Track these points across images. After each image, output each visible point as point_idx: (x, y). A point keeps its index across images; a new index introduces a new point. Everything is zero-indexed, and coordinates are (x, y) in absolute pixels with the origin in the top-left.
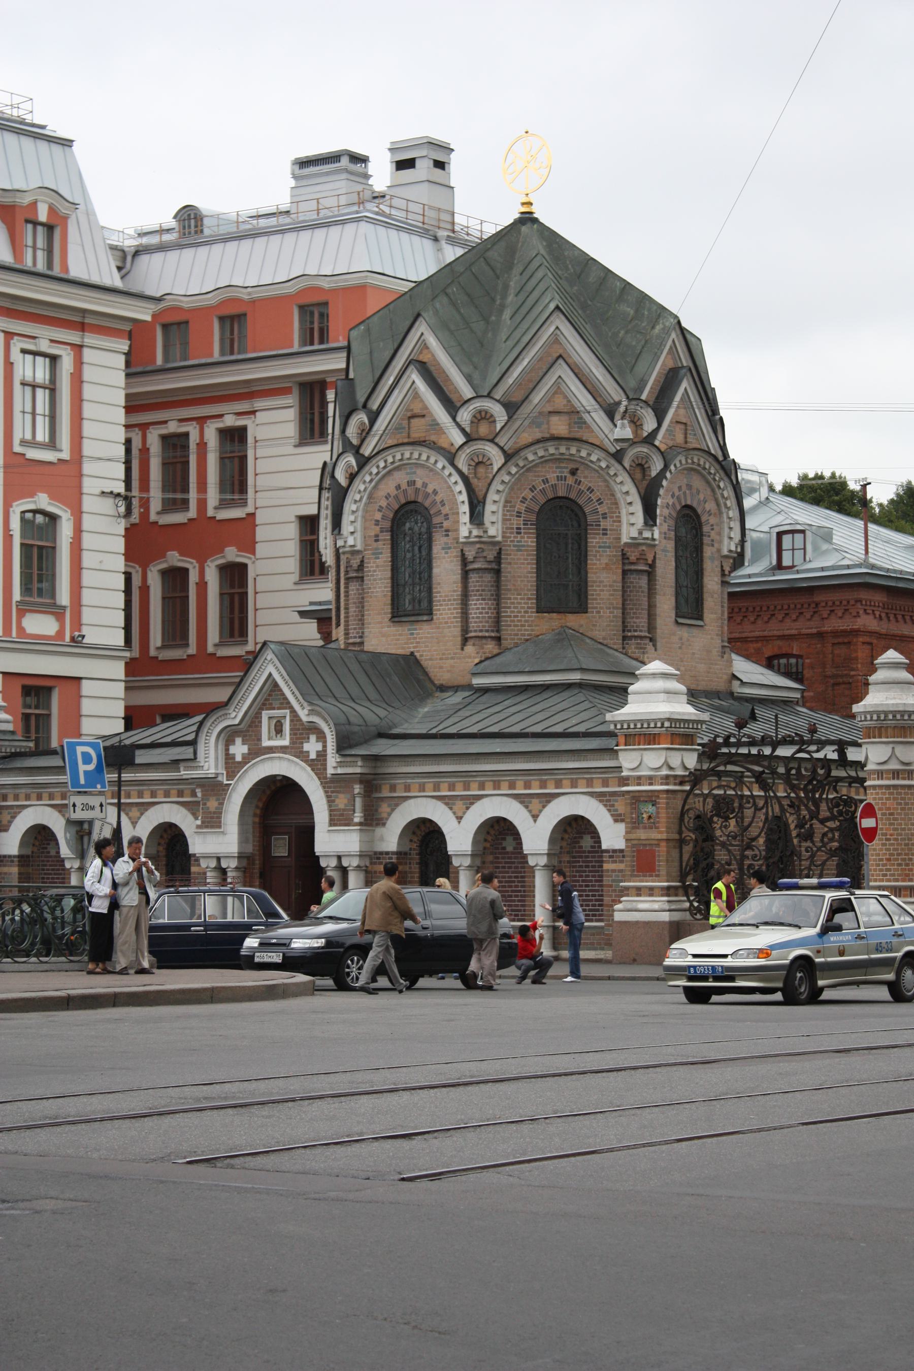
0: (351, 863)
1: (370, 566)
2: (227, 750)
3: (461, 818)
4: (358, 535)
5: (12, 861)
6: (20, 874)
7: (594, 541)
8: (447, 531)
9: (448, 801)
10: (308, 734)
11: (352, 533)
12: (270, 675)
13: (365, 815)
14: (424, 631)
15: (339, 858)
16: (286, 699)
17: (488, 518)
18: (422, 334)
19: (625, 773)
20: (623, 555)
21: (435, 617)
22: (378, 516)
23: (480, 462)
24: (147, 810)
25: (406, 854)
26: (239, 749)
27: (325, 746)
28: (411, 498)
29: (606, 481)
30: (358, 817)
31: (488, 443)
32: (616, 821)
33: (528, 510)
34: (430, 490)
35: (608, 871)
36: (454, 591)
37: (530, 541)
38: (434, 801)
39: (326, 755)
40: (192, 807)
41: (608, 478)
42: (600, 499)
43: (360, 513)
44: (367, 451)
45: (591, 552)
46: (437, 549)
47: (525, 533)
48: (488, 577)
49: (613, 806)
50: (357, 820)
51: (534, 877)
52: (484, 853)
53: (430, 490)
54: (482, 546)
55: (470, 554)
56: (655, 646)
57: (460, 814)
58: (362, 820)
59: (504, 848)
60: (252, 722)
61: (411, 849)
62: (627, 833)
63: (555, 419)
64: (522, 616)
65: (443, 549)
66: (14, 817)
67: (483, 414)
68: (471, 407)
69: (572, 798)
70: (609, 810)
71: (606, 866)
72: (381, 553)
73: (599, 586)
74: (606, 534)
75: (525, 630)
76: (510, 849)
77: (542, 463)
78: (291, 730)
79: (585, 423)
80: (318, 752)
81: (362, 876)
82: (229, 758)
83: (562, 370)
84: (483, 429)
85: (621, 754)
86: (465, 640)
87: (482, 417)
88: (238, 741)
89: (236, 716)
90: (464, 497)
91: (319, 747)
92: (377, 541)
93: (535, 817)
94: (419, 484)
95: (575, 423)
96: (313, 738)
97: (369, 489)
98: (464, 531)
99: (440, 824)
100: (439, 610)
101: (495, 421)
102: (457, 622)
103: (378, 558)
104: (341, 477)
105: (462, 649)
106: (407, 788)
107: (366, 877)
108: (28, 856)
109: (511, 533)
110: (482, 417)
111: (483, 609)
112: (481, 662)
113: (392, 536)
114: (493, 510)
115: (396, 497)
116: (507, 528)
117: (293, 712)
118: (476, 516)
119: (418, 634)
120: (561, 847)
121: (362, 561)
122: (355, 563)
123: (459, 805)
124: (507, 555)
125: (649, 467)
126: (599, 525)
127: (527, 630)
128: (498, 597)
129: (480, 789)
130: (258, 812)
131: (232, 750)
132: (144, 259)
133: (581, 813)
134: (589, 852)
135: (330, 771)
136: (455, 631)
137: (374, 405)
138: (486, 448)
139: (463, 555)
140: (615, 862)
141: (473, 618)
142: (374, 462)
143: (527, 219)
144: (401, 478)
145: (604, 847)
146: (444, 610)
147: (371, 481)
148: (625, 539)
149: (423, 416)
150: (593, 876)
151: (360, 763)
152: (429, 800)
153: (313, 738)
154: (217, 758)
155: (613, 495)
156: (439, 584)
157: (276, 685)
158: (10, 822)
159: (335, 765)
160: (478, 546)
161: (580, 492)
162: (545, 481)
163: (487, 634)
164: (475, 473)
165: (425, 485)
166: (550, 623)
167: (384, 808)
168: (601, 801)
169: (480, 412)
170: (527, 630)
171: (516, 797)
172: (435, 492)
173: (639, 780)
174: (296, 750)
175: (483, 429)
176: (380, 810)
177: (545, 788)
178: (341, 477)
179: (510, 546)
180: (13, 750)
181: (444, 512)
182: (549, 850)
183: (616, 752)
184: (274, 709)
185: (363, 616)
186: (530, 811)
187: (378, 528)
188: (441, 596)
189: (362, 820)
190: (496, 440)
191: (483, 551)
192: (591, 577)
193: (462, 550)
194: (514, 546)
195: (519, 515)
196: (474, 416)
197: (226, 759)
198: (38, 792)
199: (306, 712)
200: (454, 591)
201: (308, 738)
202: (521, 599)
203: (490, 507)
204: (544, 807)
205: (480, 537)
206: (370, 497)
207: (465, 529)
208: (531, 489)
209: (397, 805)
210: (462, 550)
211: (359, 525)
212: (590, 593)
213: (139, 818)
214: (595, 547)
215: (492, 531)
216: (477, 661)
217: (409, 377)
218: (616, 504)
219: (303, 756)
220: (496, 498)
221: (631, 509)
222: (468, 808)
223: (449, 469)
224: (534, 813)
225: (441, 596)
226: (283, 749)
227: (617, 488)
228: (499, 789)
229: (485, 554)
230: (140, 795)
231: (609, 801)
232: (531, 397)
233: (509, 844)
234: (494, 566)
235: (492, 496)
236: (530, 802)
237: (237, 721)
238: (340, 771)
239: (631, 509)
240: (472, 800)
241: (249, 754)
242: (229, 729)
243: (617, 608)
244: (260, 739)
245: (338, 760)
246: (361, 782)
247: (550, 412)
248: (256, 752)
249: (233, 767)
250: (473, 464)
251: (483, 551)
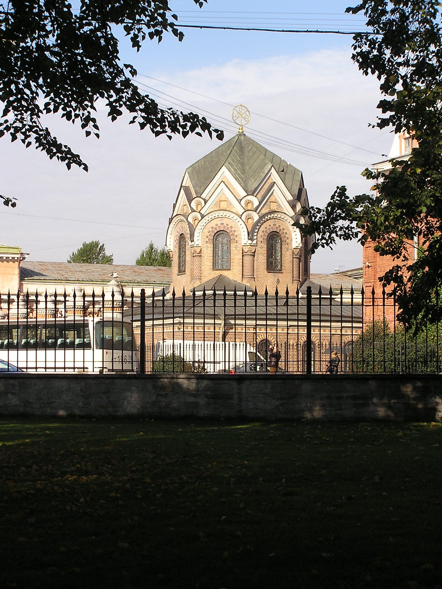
4: (200, 241)
53: (229, 226)
55: (246, 250)
87: (248, 202)
94: (225, 224)
110: (248, 202)
137: (203, 196)
144: (218, 222)
148: (294, 247)
175: (249, 207)
207: (244, 239)
211: (200, 238)
223: (239, 219)
234: (252, 254)
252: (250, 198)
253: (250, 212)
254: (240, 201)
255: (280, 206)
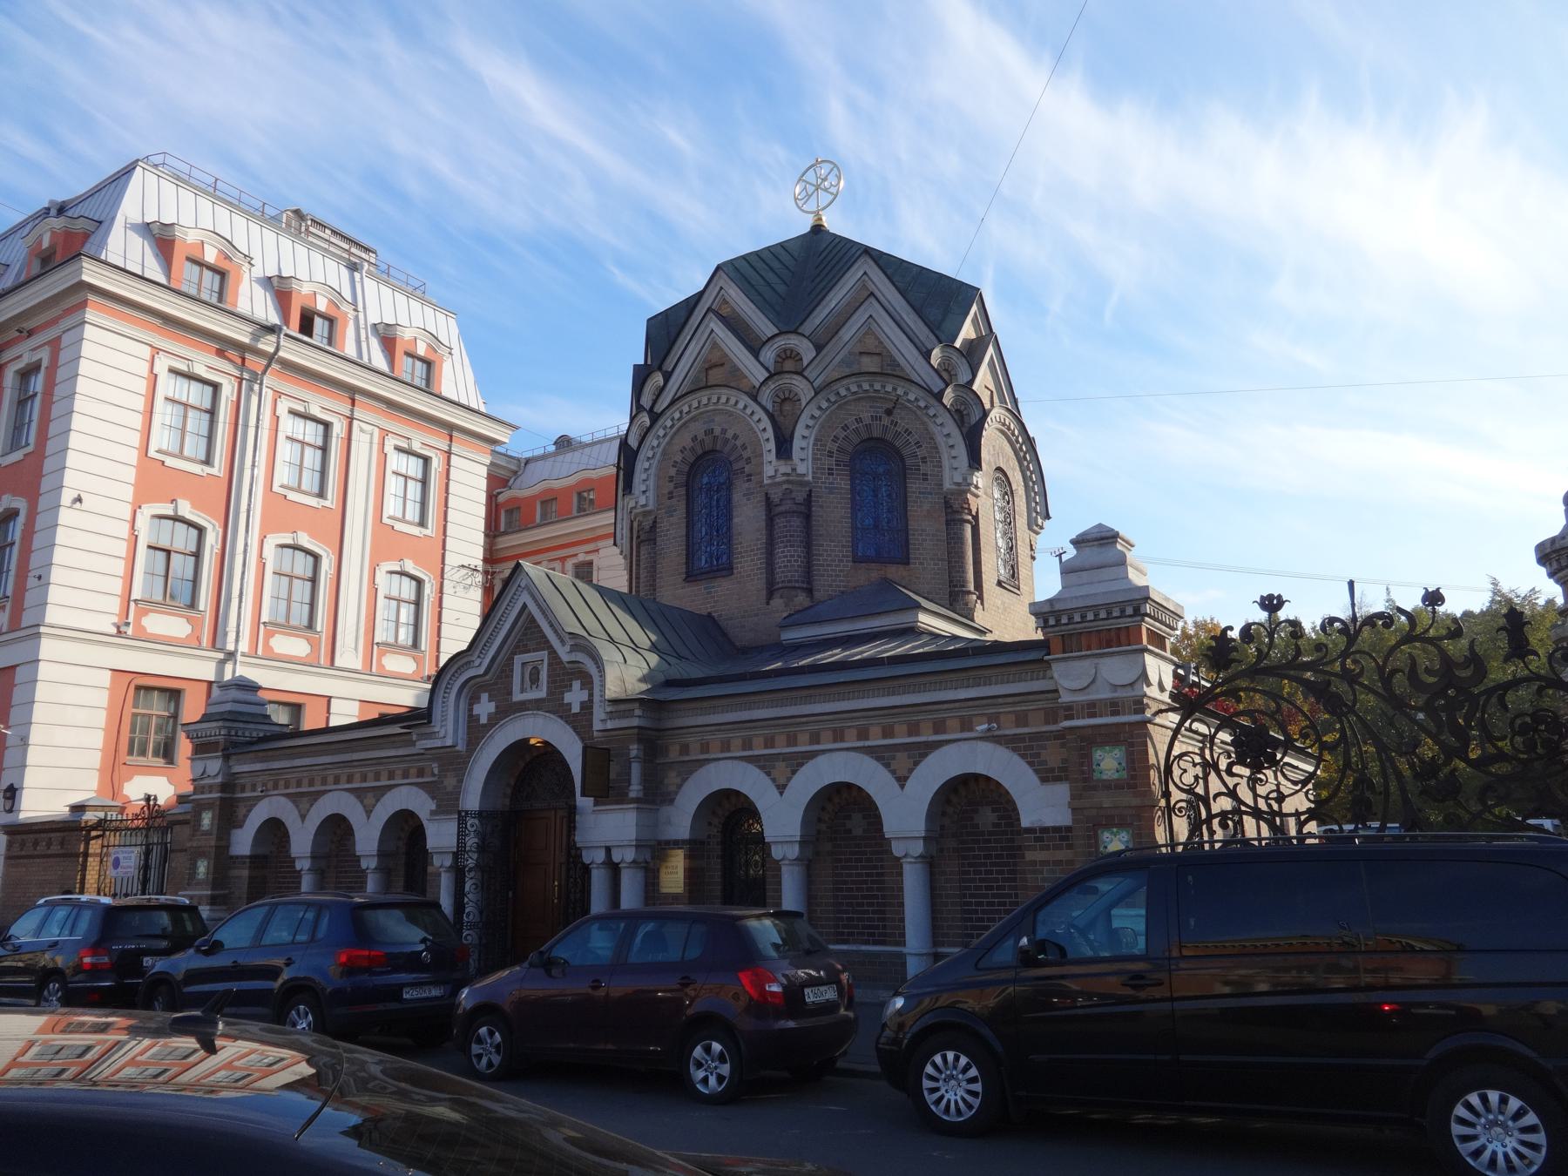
0: (625, 855)
1: (663, 525)
2: (471, 710)
3: (784, 786)
4: (651, 494)
5: (244, 863)
6: (250, 877)
7: (914, 486)
8: (750, 475)
9: (764, 763)
10: (571, 680)
11: (644, 492)
12: (525, 606)
13: (645, 788)
14: (723, 587)
15: (608, 850)
16: (544, 636)
17: (796, 453)
18: (721, 288)
19: (1065, 698)
20: (946, 502)
21: (735, 571)
22: (673, 472)
23: (787, 399)
24: (383, 795)
25: (702, 843)
26: (485, 708)
27: (591, 695)
28: (708, 446)
29: (924, 423)
30: (635, 789)
31: (795, 376)
32: (1044, 780)
33: (840, 450)
34: (729, 435)
35: (1034, 863)
36: (758, 539)
37: (843, 483)
38: (744, 764)
39: (592, 707)
40: (431, 789)
41: (926, 419)
42: (918, 442)
43: (652, 471)
44: (658, 408)
45: (911, 497)
46: (737, 497)
47: (838, 475)
48: (797, 522)
49: (1038, 755)
50: (632, 795)
51: (901, 874)
52: (817, 840)
53: (729, 435)
54: (790, 486)
55: (776, 496)
56: (982, 604)
57: (782, 781)
58: (641, 795)
59: (850, 831)
60: (502, 671)
61: (709, 837)
62: (1073, 797)
63: (866, 360)
64: (836, 566)
65: (744, 495)
66: (249, 811)
67: (788, 353)
68: (776, 346)
69: (965, 746)
70: (1031, 764)
71: (1030, 856)
72: (675, 510)
73: (921, 535)
74: (927, 479)
75: (840, 581)
76: (858, 832)
77: (855, 400)
78: (549, 676)
79: (899, 365)
80: (582, 703)
81: (640, 875)
82: (472, 719)
83: (872, 308)
84: (789, 365)
85: (1054, 666)
86: (770, 594)
87: (788, 355)
88: (485, 697)
89: (480, 665)
90: (770, 433)
91: (584, 696)
92: (669, 498)
93: (902, 781)
94: (717, 431)
95: (888, 365)
96: (576, 685)
97: (662, 447)
98: (769, 471)
99: (752, 796)
100: (741, 563)
101: (801, 359)
102: (761, 573)
103: (672, 516)
104: (633, 442)
105: (768, 604)
106: (705, 748)
107: (646, 878)
108: (265, 857)
109: (822, 474)
110: (788, 355)
111: (792, 556)
112: (790, 615)
113: (687, 491)
114: (802, 442)
115: (692, 449)
116: (817, 468)
117: (553, 653)
118: (784, 448)
119: (717, 592)
120: (942, 827)
121: (655, 522)
122: (647, 524)
123: (781, 768)
124: (817, 497)
125: (968, 415)
126: (919, 470)
127: (843, 581)
128: (808, 545)
129: (811, 743)
130: (509, 791)
131: (477, 709)
132: (531, 466)
133: (980, 769)
134: (990, 833)
135: (597, 726)
136: (758, 583)
137: (668, 366)
138: (794, 382)
139: (767, 498)
140: (1047, 848)
141: (780, 567)
142: (668, 414)
143: (818, 229)
144: (698, 429)
145: (1025, 822)
146: (746, 561)
147: (665, 435)
149: (722, 365)
150: (998, 872)
151: (638, 712)
152: (735, 762)
153: (576, 685)
154: (456, 721)
155: (932, 438)
156: (740, 534)
157: (532, 620)
158: (246, 816)
159: (603, 716)
160: (785, 486)
161: (897, 434)
162: (859, 420)
163: (797, 585)
164: (781, 411)
165: (724, 431)
166: (868, 575)
167: (672, 778)
168: (1014, 750)
169: (785, 351)
170: (843, 581)
171: (871, 751)
172: (735, 437)
173: (1092, 709)
174: (554, 706)
176: (666, 781)
177: (917, 734)
178: (633, 442)
179: (821, 487)
180: (261, 735)
181: (745, 456)
182: (927, 831)
183: (1048, 662)
184: (529, 651)
185: (654, 580)
186: (893, 772)
187: (672, 485)
188: (742, 547)
189: (641, 795)
190: (806, 374)
191: (791, 491)
192: (912, 525)
193: (767, 494)
194: (826, 488)
195: (830, 454)
196: (779, 356)
197: (469, 722)
198: (275, 782)
199: (567, 648)
200: (758, 539)
201: (571, 686)
202: (835, 546)
203: (797, 443)
204: (916, 764)
205: (788, 475)
206: (664, 453)
207: (771, 467)
208: (842, 428)
209: (691, 773)
210: (767, 494)
211: (651, 483)
212: (911, 542)
213: (374, 806)
214: (914, 492)
215: (801, 469)
216: (785, 614)
217: (707, 326)
218: (937, 448)
219: (563, 712)
220: (806, 433)
221: (954, 453)
222: (794, 772)
223: (753, 406)
224: (899, 774)
225: (742, 547)
226: (537, 705)
227: (935, 430)
228: (842, 740)
229: (794, 495)
230: (377, 778)
231: (1032, 748)
232: (841, 333)
233: (857, 825)
234: (802, 508)
235: (800, 431)
236: (894, 758)
237: (481, 671)
238: (610, 725)
239: (954, 453)
240: (798, 761)
241: (496, 713)
242: (472, 682)
243: (942, 560)
244: (510, 693)
245: (608, 709)
246: (640, 741)
247: (861, 353)
248: (505, 709)
249: (476, 732)
250: (779, 400)
251: (791, 491)
252: (792, 341)
253: (786, 380)
254: (755, 352)
255: (896, 365)
